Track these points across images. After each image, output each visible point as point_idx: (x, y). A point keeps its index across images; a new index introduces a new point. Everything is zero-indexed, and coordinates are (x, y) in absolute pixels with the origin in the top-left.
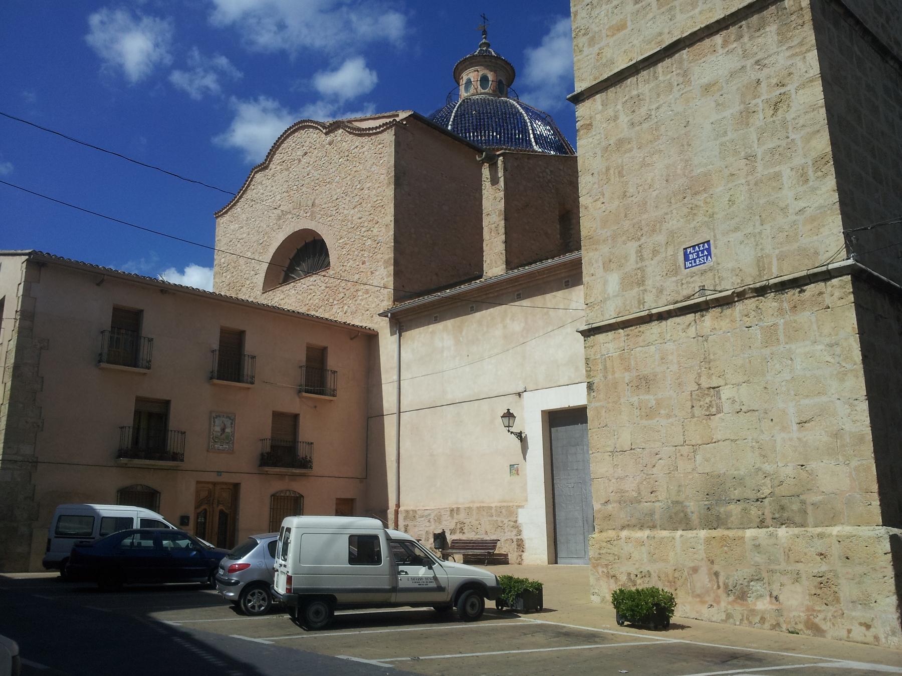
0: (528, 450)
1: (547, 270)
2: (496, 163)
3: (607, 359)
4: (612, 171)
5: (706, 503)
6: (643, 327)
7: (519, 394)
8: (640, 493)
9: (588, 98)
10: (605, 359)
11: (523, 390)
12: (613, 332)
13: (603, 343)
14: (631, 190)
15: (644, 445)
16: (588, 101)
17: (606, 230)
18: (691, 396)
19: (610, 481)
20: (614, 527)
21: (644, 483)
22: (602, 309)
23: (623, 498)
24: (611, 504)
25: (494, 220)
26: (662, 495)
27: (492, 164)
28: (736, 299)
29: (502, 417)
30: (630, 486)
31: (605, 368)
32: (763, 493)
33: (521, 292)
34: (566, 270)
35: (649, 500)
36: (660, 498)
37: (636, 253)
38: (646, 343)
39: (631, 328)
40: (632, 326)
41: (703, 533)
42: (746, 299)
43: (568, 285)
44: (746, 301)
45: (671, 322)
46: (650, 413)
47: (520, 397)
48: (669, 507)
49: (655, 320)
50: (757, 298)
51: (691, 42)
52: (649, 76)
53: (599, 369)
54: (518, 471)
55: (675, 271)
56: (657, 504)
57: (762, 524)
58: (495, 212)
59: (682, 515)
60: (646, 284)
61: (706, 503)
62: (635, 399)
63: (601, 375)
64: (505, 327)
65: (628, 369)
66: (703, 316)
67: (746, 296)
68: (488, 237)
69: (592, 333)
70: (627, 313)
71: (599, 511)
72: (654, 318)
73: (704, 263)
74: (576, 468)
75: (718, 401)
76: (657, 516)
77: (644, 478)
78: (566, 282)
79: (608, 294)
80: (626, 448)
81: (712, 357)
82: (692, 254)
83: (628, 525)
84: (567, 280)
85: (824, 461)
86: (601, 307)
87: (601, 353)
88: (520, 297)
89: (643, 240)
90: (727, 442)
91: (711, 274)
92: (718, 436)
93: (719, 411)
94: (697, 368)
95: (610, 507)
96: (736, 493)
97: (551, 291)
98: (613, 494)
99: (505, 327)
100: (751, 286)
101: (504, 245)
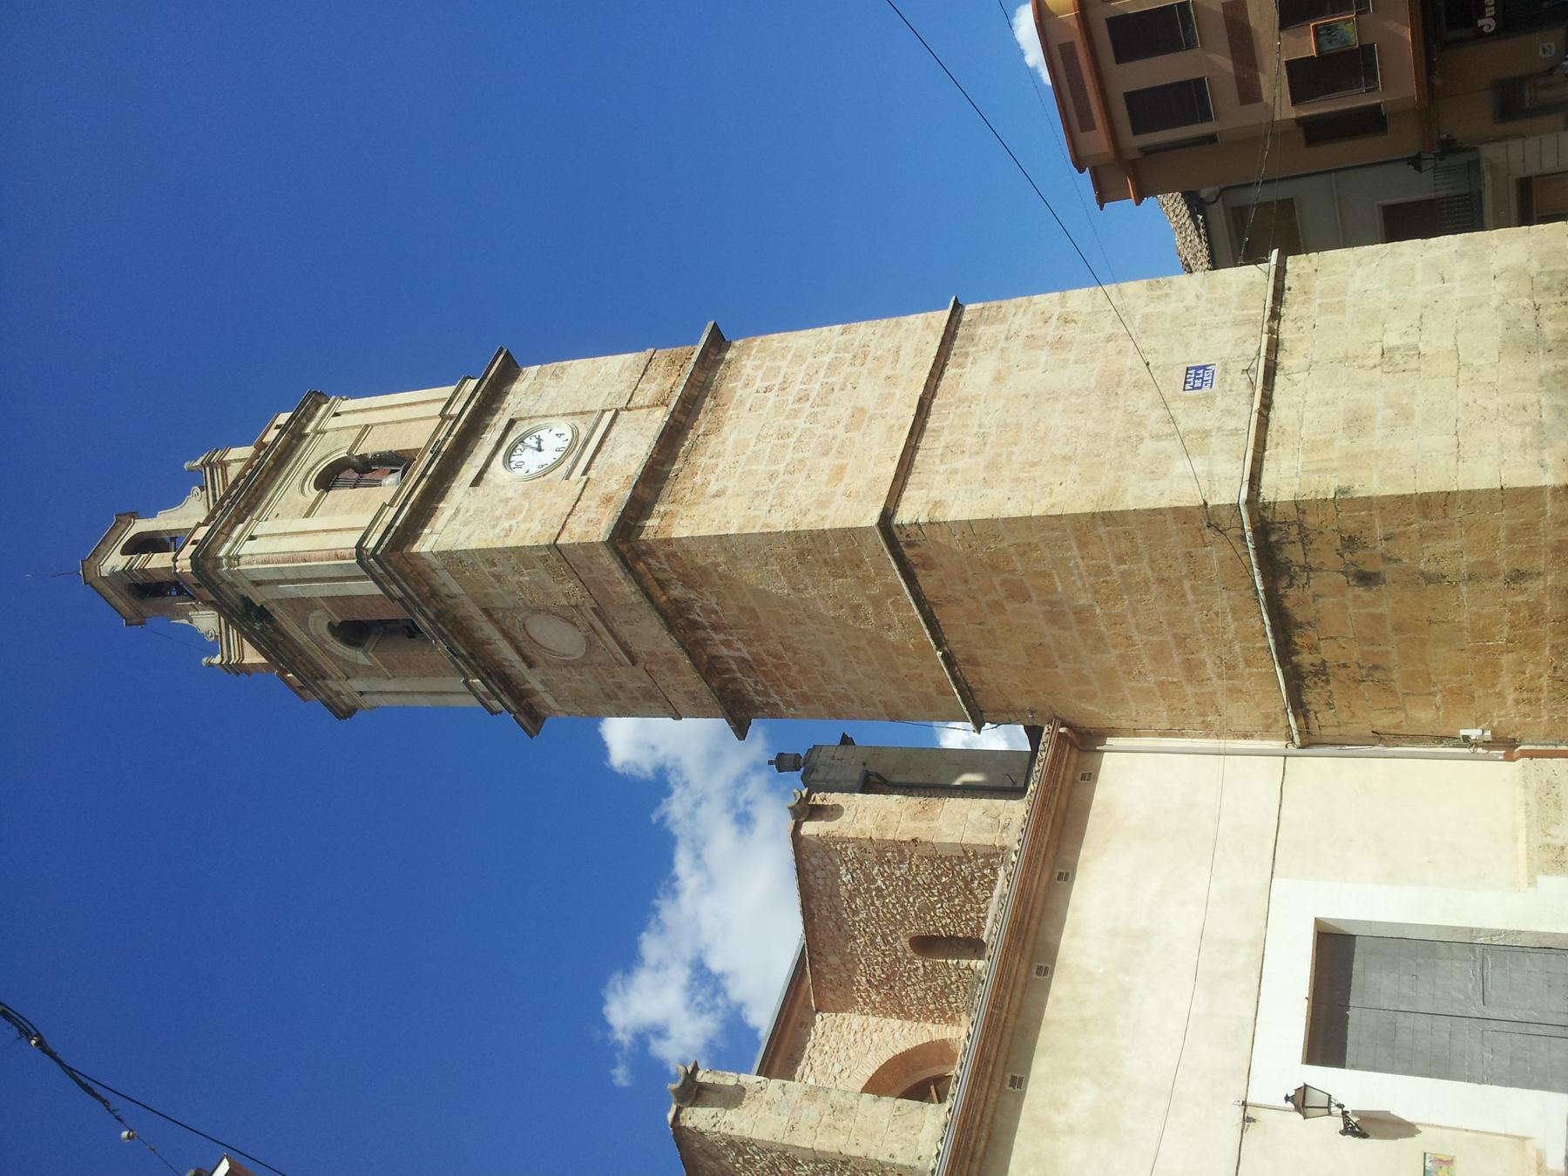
0: (1392, 1113)
1: (999, 987)
2: (703, 1088)
3: (1305, 469)
4: (1022, 475)
5: (1541, 353)
6: (1273, 426)
7: (1248, 1120)
8: (1527, 424)
9: (897, 505)
12: (1265, 462)
14: (1067, 450)
15: (1452, 421)
17: (1104, 478)
18: (1389, 373)
22: (1223, 479)
24: (1544, 460)
25: (814, 1114)
26: (1531, 398)
29: (1305, 1118)
30: (1514, 436)
31: (1319, 470)
32: (1528, 304)
33: (1008, 1076)
34: (1018, 955)
36: (1535, 399)
38: (1297, 421)
39: (1268, 442)
40: (1265, 441)
43: (1046, 968)
45: (1278, 397)
46: (1406, 415)
47: (1254, 1120)
48: (1549, 390)
49: (1268, 414)
50: (1282, 322)
51: (931, 394)
52: (931, 436)
54: (1440, 1160)
55: (1213, 397)
56: (1544, 402)
58: (801, 1108)
59: (1559, 376)
60: (1210, 428)
61: (1541, 353)
63: (1328, 476)
64: (1071, 1130)
65: (1329, 443)
67: (1276, 328)
68: (842, 1138)
69: (1255, 487)
70: (1243, 449)
71: (1557, 475)
72: (1265, 413)
73: (1213, 372)
74: (1447, 1036)
75: (1402, 350)
77: (1504, 419)
78: (1038, 973)
79: (1203, 471)
81: (1342, 355)
82: (1194, 383)
84: (1034, 971)
85: (1491, 261)
86: (1219, 480)
87: (1292, 477)
88: (1021, 1079)
89: (1145, 434)
91: (1232, 364)
92: (1450, 344)
93: (1416, 347)
94: (1351, 369)
95: (1549, 460)
96: (1529, 327)
97: (1041, 1006)
99: (1071, 1130)
100: (1266, 319)
101: (885, 1098)
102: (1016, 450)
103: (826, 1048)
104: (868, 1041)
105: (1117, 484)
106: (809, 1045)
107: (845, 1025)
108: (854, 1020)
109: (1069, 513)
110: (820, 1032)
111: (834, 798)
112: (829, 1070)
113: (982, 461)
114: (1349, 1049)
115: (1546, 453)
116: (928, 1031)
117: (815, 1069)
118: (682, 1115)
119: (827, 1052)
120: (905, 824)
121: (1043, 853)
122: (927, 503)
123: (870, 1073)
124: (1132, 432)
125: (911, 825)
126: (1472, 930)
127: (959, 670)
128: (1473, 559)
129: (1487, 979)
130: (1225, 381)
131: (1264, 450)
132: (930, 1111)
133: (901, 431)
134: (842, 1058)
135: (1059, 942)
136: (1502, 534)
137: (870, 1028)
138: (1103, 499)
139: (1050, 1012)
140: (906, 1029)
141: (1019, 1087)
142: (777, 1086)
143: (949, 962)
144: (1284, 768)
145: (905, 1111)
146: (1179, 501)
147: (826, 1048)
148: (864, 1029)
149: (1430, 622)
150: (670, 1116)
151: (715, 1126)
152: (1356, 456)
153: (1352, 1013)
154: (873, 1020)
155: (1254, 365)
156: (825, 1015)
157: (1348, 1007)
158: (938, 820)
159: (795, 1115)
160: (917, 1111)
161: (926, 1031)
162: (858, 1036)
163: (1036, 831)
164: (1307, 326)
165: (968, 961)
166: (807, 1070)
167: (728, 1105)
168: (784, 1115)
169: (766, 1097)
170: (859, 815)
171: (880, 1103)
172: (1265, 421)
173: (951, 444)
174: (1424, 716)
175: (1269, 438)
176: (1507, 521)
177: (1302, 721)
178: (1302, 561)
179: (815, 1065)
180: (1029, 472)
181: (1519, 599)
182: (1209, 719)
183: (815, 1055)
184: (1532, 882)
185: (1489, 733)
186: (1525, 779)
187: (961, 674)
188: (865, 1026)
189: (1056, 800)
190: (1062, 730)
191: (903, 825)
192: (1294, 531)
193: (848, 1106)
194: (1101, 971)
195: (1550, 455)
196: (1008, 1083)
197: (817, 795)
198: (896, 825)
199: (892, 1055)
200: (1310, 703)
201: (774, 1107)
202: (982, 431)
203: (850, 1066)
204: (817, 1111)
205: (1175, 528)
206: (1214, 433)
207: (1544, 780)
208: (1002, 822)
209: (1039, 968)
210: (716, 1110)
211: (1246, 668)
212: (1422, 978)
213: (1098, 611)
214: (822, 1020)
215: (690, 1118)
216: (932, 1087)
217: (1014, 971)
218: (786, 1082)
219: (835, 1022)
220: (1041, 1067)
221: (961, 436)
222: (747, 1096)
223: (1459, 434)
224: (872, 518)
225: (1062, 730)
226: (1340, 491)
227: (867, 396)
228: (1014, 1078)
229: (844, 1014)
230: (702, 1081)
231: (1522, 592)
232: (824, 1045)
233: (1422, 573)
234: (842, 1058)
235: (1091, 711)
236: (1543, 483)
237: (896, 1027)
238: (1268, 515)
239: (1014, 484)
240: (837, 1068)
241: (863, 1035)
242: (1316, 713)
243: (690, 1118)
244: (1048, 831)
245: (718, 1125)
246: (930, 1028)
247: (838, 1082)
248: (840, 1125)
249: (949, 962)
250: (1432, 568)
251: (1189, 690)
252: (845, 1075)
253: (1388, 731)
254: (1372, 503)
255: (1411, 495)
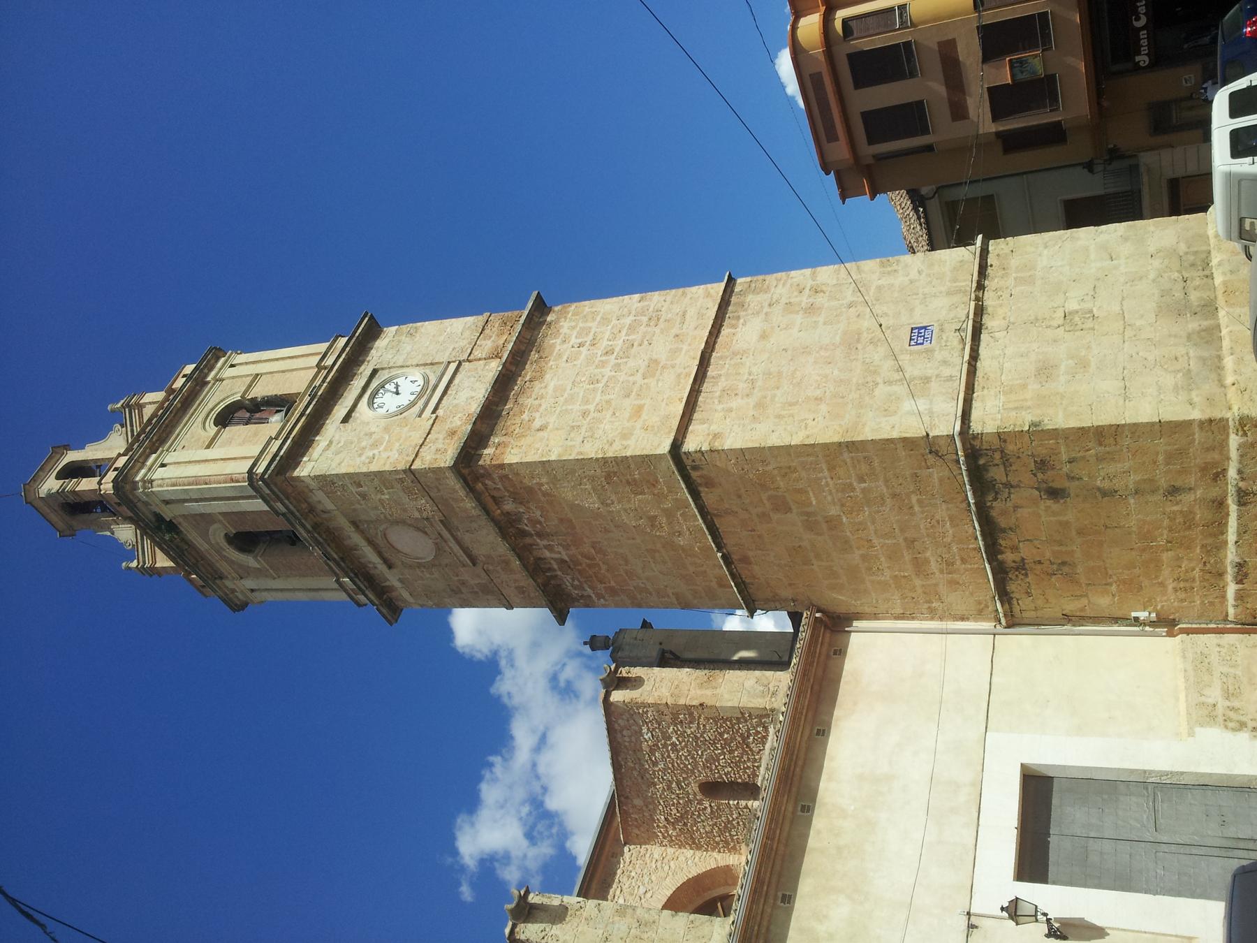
0: (1086, 919)
1: (771, 823)
2: (534, 907)
3: (1005, 407)
4: (783, 413)
5: (1188, 315)
6: (979, 373)
7: (971, 927)
9: (684, 437)
10: (1004, 409)
11: (965, 918)
12: (974, 402)
13: (984, 411)
14: (818, 393)
16: (687, 438)
18: (1070, 331)
19: (1162, 400)
20: (1222, 394)
21: (1166, 367)
22: (941, 416)
23: (1185, 388)
25: (624, 928)
26: (1182, 350)
27: (529, 913)
28: (981, 303)
30: (1169, 381)
31: (1016, 408)
33: (780, 895)
34: (786, 796)
35: (1186, 362)
37: (890, 385)
39: (976, 386)
40: (974, 385)
41: (1221, 313)
42: (983, 298)
44: (985, 299)
45: (983, 351)
46: (1083, 364)
47: (977, 927)
48: (1195, 345)
50: (985, 292)
52: (711, 382)
53: (1015, 415)
55: (932, 351)
56: (1192, 354)
57: (1211, 277)
58: (613, 923)
59: (1203, 333)
60: (930, 375)
61: (1188, 315)
62: (1062, 379)
63: (1024, 413)
65: (1024, 386)
66: (987, 328)
67: (981, 296)
69: (967, 422)
72: (973, 363)
74: (1128, 856)
75: (1080, 313)
76: (1206, 354)
79: (926, 410)
80: (1122, 384)
81: (1033, 318)
83: (1220, 381)
84: (799, 809)
85: (1149, 243)
87: (996, 414)
88: (790, 897)
89: (879, 380)
90: (1124, 303)
91: (946, 325)
92: (1117, 308)
93: (1091, 311)
94: (1040, 329)
95: (1196, 399)
96: (1179, 295)
97: (805, 837)
98: (1180, 397)
100: (973, 290)
101: (681, 914)
102: (778, 393)
103: (633, 874)
104: (666, 868)
105: (858, 420)
106: (619, 872)
107: (648, 855)
108: (656, 851)
109: (820, 442)
110: (628, 861)
111: (637, 671)
112: (636, 891)
113: (752, 401)
114: (1051, 868)
115: (1194, 394)
116: (715, 858)
117: (624, 890)
118: (517, 930)
119: (633, 877)
120: (694, 692)
121: (804, 714)
122: (708, 435)
123: (669, 893)
124: (869, 379)
125: (699, 692)
126: (1145, 772)
127: (735, 568)
128: (1138, 478)
129: (1158, 811)
130: (942, 338)
131: (973, 393)
132: (717, 923)
133: (687, 378)
134: (646, 882)
135: (818, 785)
136: (1161, 458)
137: (668, 857)
138: (847, 431)
139: (812, 842)
140: (697, 858)
141: (789, 903)
142: (593, 906)
143: (731, 802)
144: (994, 644)
145: (697, 924)
146: (907, 433)
147: (633, 874)
148: (663, 858)
149: (1106, 527)
150: (507, 931)
151: (543, 938)
152: (1045, 397)
153: (1053, 840)
154: (670, 850)
155: (964, 325)
156: (632, 847)
157: (1049, 835)
158: (720, 687)
159: (608, 928)
160: (708, 924)
161: (713, 859)
162: (659, 864)
163: (798, 696)
164: (1006, 295)
165: (746, 802)
166: (618, 892)
167: (555, 920)
168: (599, 928)
169: (585, 914)
170: (657, 685)
171: (677, 918)
172: (973, 369)
173: (727, 388)
174: (1103, 602)
175: (976, 383)
176: (1165, 448)
177: (1007, 606)
178: (1004, 480)
179: (624, 888)
180: (789, 410)
181: (1175, 508)
182: (934, 605)
183: (624, 879)
184: (1191, 734)
185: (1155, 615)
186: (1184, 651)
187: (737, 570)
188: (664, 855)
189: (814, 671)
190: (818, 615)
191: (693, 692)
192: (997, 456)
193: (651, 921)
194: (852, 808)
195: (1197, 396)
196: (780, 901)
197: (623, 669)
198: (686, 692)
199: (686, 878)
200: (1013, 592)
201: (591, 923)
202: (751, 378)
203: (652, 888)
204: (626, 925)
205: (904, 453)
206: (933, 379)
207: (1199, 652)
208: (771, 689)
209: (803, 807)
210: (544, 925)
211: (961, 564)
212: (1107, 810)
213: (844, 520)
214: (629, 851)
215: (523, 933)
216: (719, 904)
217: (783, 808)
218: (601, 902)
219: (640, 852)
220: (806, 886)
221: (735, 382)
222: (569, 913)
223: (1125, 379)
224: (664, 447)
225: (818, 615)
226: (1033, 424)
227: (661, 349)
228: (784, 896)
229: (647, 846)
230: (533, 902)
231: (1177, 504)
232: (631, 872)
233: (1099, 489)
234: (646, 882)
235: (841, 600)
236: (1192, 417)
237: (689, 856)
238: (977, 443)
239: (777, 420)
240: (642, 890)
241: (662, 863)
242: (1018, 600)
243: (523, 933)
244: (808, 696)
245: (546, 937)
246: (716, 856)
247: (643, 901)
248: (645, 936)
249: (731, 802)
250: (1106, 485)
251: (918, 582)
252: (649, 895)
253: (1075, 614)
254: (1058, 434)
255: (1089, 427)
